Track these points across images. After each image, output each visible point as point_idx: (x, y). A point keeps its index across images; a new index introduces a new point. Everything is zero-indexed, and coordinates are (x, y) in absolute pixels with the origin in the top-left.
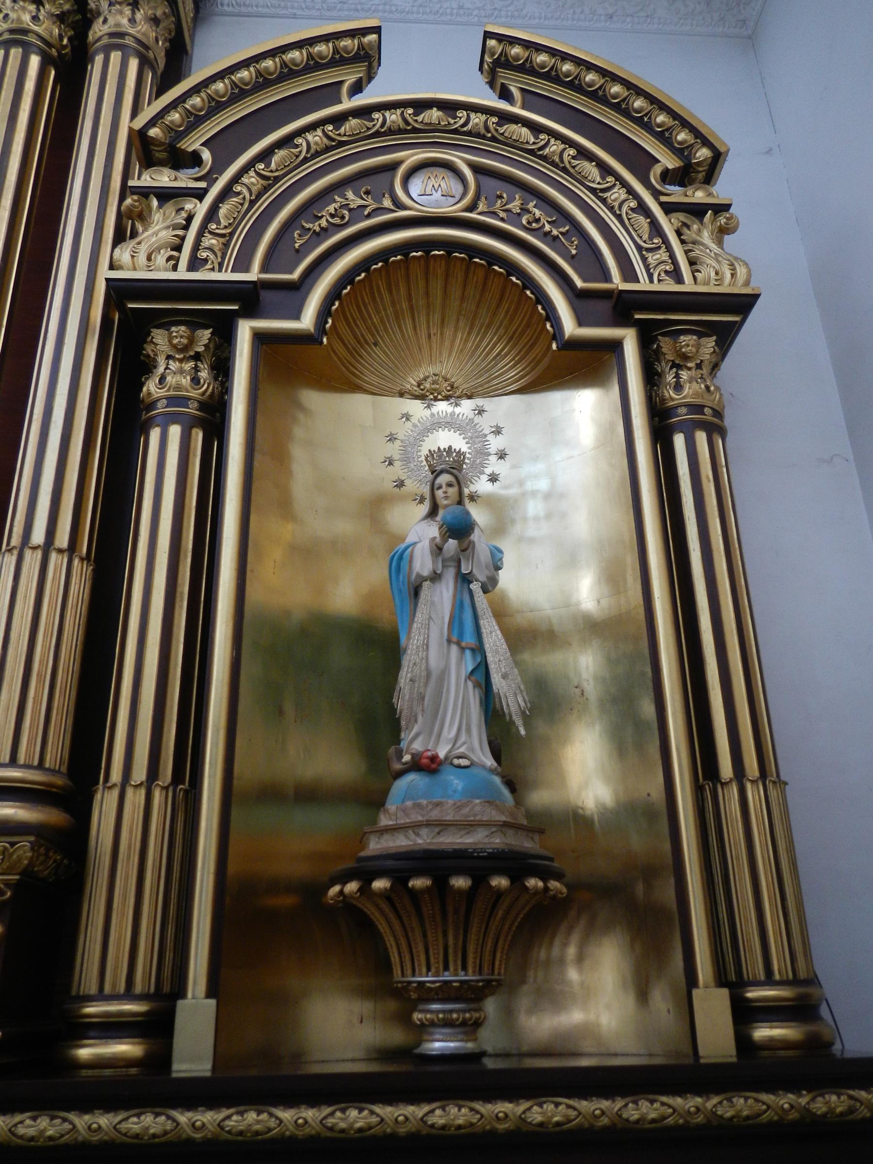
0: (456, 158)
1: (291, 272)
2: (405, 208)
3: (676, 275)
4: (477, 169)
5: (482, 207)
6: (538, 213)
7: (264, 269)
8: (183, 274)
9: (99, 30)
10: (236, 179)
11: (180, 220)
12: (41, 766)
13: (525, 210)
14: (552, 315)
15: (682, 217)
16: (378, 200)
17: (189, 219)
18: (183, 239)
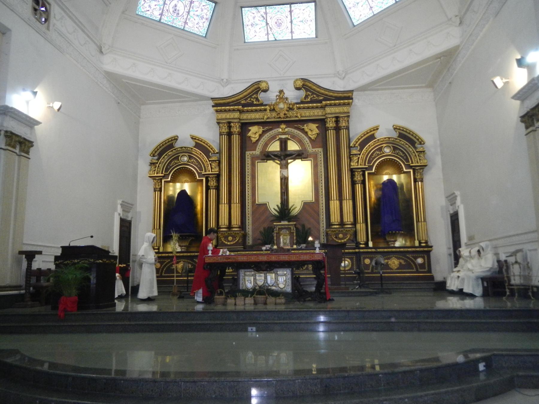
0: (390, 145)
1: (371, 164)
2: (384, 153)
3: (418, 162)
4: (393, 146)
5: (393, 152)
6: (401, 153)
7: (368, 164)
8: (359, 166)
9: (340, 125)
10: (364, 152)
11: (357, 158)
12: (350, 222)
13: (399, 152)
14: (402, 168)
15: (420, 153)
16: (380, 152)
17: (359, 158)
18: (358, 161)
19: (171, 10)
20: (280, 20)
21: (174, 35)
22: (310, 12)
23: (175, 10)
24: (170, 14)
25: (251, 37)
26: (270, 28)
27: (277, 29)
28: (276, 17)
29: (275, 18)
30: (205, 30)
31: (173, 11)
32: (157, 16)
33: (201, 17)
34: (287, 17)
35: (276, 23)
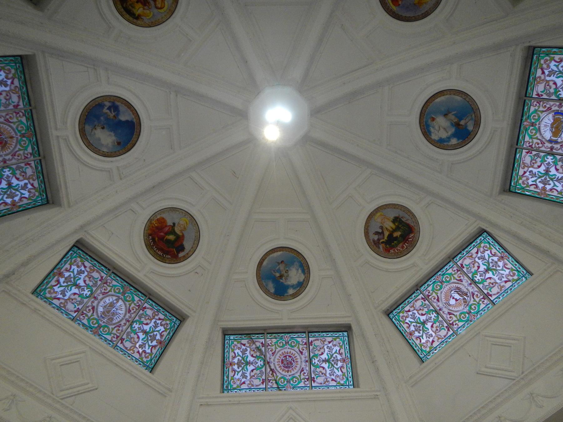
19: (101, 309)
20: (290, 357)
21: (90, 348)
22: (341, 347)
23: (108, 312)
24: (95, 316)
25: (235, 386)
26: (271, 370)
27: (283, 373)
28: (283, 351)
29: (280, 353)
30: (153, 361)
31: (104, 313)
32: (71, 313)
33: (150, 336)
34: (302, 353)
35: (282, 363)
